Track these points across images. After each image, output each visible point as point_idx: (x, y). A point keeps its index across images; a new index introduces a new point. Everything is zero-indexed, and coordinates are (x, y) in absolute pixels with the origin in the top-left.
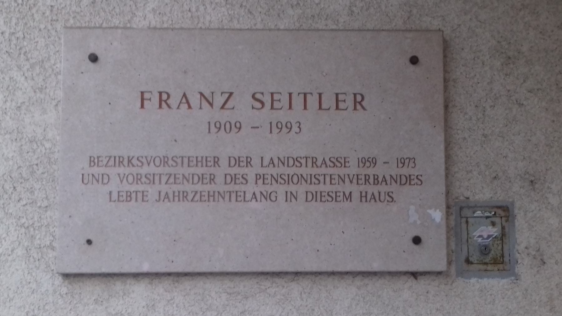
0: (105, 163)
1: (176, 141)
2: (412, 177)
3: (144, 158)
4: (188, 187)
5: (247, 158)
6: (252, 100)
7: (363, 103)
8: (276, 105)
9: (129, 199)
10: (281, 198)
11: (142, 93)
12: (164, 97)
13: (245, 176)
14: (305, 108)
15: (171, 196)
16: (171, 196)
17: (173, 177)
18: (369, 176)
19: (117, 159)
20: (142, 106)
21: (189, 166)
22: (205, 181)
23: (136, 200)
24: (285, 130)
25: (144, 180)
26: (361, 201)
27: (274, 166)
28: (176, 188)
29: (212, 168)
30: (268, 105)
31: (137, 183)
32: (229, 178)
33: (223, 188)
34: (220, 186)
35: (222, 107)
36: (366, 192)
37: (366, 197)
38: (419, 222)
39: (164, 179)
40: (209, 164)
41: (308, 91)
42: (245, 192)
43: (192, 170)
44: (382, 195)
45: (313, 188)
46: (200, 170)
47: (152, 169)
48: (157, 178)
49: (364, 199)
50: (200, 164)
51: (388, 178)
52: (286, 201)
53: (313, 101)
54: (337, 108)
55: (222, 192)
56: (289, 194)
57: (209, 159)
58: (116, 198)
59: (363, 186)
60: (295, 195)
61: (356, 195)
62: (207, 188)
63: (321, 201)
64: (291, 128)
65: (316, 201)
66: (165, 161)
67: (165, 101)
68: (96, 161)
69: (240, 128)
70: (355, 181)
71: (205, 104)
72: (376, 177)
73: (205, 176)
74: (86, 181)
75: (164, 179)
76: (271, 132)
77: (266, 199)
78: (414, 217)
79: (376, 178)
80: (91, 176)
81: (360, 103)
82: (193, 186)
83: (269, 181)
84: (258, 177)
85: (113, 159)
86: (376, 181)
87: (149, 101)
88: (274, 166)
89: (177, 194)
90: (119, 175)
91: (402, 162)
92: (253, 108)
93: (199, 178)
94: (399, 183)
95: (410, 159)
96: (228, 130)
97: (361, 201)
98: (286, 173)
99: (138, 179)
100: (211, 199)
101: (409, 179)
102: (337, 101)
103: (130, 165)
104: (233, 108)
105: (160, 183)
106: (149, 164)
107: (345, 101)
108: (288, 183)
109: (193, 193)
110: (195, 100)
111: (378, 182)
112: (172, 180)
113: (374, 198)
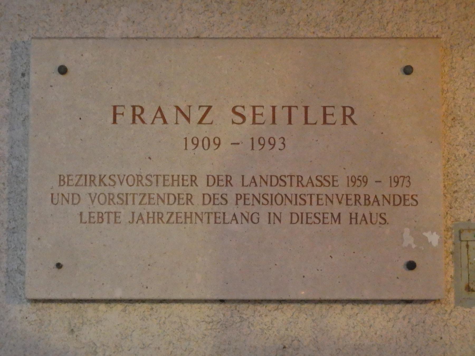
0: (75, 182)
1: (150, 158)
4: (164, 208)
5: (227, 176)
6: (232, 113)
7: (353, 117)
8: (258, 119)
9: (100, 220)
10: (264, 220)
11: (115, 107)
12: (138, 111)
13: (224, 196)
14: (290, 122)
15: (145, 217)
16: (145, 217)
17: (147, 197)
19: (88, 177)
20: (115, 122)
21: (164, 185)
22: (181, 202)
24: (268, 146)
25: (116, 200)
26: (351, 223)
27: (256, 185)
28: (150, 208)
29: (189, 187)
30: (249, 119)
31: (109, 204)
32: (207, 197)
33: (201, 209)
35: (200, 122)
36: (357, 214)
38: (414, 246)
40: (186, 183)
41: (293, 104)
42: (224, 213)
44: (374, 216)
45: (298, 209)
46: (176, 190)
47: (125, 188)
48: (130, 198)
49: (354, 221)
50: (176, 183)
51: (380, 198)
52: (269, 223)
53: (298, 114)
54: (325, 122)
55: (199, 213)
56: (272, 215)
57: (185, 178)
58: (87, 219)
59: (353, 207)
60: (279, 216)
61: (345, 218)
63: (307, 223)
64: (274, 145)
65: (302, 223)
66: (138, 180)
67: (139, 116)
68: (66, 180)
69: (219, 145)
70: (344, 201)
71: (181, 119)
72: (367, 197)
73: (181, 196)
74: (55, 201)
76: (253, 149)
77: (247, 220)
78: (409, 240)
79: (367, 198)
80: (60, 196)
81: (349, 117)
82: (169, 206)
83: (251, 201)
84: (239, 197)
85: (83, 178)
86: (367, 202)
87: (121, 116)
88: (256, 185)
89: (151, 215)
90: (90, 194)
91: (396, 181)
92: (233, 122)
93: (175, 198)
94: (392, 204)
95: (404, 177)
96: (206, 147)
97: (351, 223)
99: (110, 199)
100: (188, 220)
101: (403, 199)
102: (325, 115)
103: (102, 184)
104: (212, 123)
105: (134, 204)
106: (121, 183)
107: (333, 115)
108: (272, 204)
109: (169, 215)
110: (170, 114)
111: (370, 202)
112: (146, 200)
113: (365, 220)
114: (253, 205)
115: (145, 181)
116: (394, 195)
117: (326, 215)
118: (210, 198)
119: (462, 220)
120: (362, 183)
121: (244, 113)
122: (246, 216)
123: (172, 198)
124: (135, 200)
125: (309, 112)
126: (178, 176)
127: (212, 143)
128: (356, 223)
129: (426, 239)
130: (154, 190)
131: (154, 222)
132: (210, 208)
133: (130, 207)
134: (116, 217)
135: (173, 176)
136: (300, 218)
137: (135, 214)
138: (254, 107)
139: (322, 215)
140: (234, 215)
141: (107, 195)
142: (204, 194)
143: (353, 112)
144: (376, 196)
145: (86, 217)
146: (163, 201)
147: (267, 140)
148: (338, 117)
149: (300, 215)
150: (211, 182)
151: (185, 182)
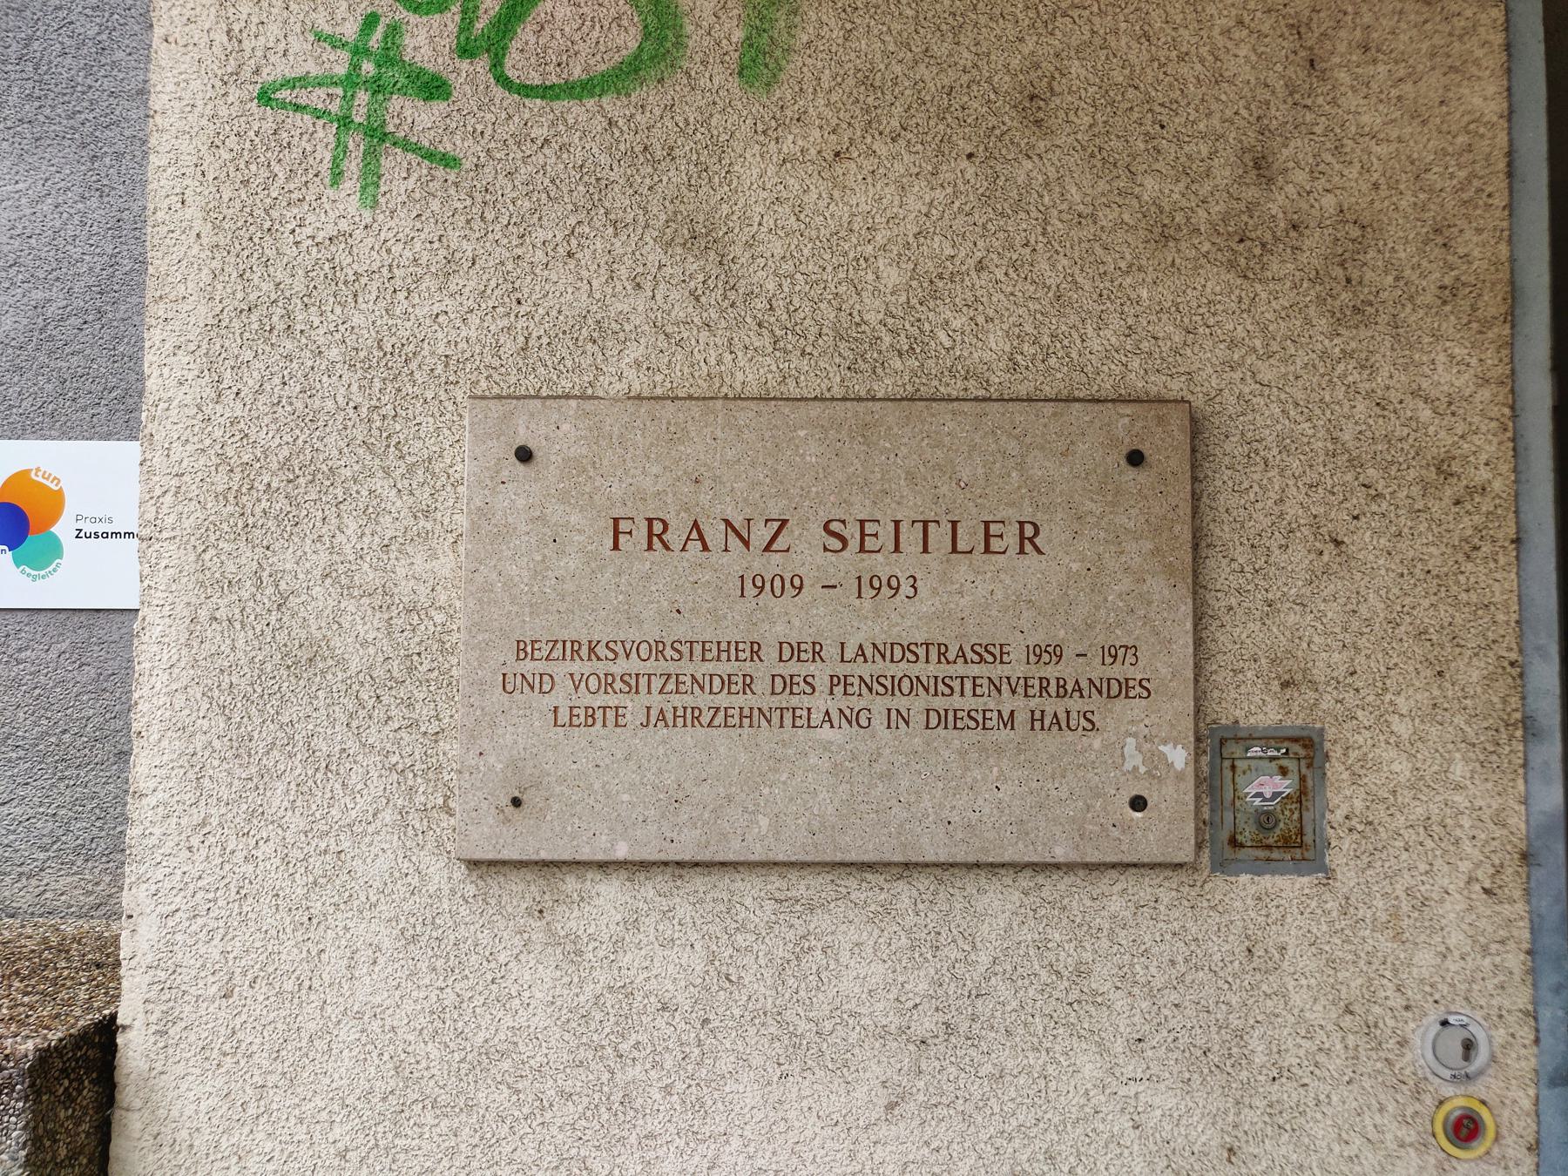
0: (545, 654)
1: (678, 611)
2: (1131, 683)
3: (619, 644)
4: (703, 700)
5: (814, 643)
6: (824, 533)
7: (1037, 541)
8: (870, 543)
9: (590, 721)
10: (879, 722)
11: (616, 521)
12: (658, 528)
13: (809, 679)
14: (925, 550)
15: (669, 716)
16: (669, 716)
17: (673, 680)
18: (1048, 681)
19: (568, 645)
20: (616, 547)
21: (703, 660)
22: (734, 688)
23: (604, 725)
24: (886, 591)
25: (618, 685)
26: (1032, 728)
27: (866, 661)
28: (677, 700)
29: (748, 664)
30: (854, 544)
31: (606, 692)
32: (778, 680)
33: (768, 702)
34: (761, 698)
35: (767, 549)
36: (1043, 712)
37: (1042, 720)
38: (1142, 770)
39: (657, 684)
40: (803, 656)
41: (931, 516)
42: (809, 709)
43: (710, 667)
44: (1074, 715)
45: (939, 703)
46: (724, 668)
47: (634, 665)
48: (643, 681)
49: (1037, 725)
50: (724, 656)
51: (1084, 684)
52: (889, 727)
53: (939, 535)
54: (987, 550)
55: (765, 710)
56: (894, 713)
57: (741, 646)
58: (567, 719)
59: (1037, 700)
60: (906, 716)
61: (1022, 718)
62: (739, 700)
63: (955, 728)
64: (897, 589)
65: (946, 728)
66: (658, 649)
67: (659, 536)
68: (529, 649)
69: (800, 588)
70: (1020, 690)
71: (734, 542)
72: (1062, 683)
73: (734, 679)
74: (509, 688)
75: (657, 684)
76: (860, 596)
77: (850, 723)
78: (1134, 759)
79: (1061, 684)
80: (519, 678)
81: (1031, 540)
82: (712, 697)
83: (856, 688)
84: (835, 679)
85: (560, 645)
86: (1061, 690)
87: (628, 536)
88: (866, 661)
89: (680, 712)
90: (571, 675)
91: (1112, 654)
92: (826, 549)
93: (723, 683)
94: (1105, 695)
95: (1127, 648)
96: (778, 592)
97: (1032, 728)
98: (889, 674)
99: (607, 683)
100: (746, 721)
101: (1125, 686)
102: (987, 536)
103: (593, 656)
104: (788, 550)
105: (649, 692)
106: (628, 656)
107: (1001, 536)
108: (893, 694)
109: (712, 711)
110: (714, 534)
111: (1066, 691)
112: (671, 686)
113: (1058, 723)
114: (860, 695)
115: (669, 652)
116: (1109, 680)
117: (978, 682)
118: (785, 683)
119: (1223, 721)
120: (1054, 658)
121: (846, 533)
122: (849, 715)
123: (717, 681)
124: (652, 686)
125: (960, 531)
126: (729, 643)
127: (788, 585)
128: (1042, 729)
129: (1163, 756)
130: (686, 667)
131: (685, 725)
132: (783, 700)
133: (643, 699)
134: (617, 716)
135: (719, 643)
136: (943, 720)
137: (652, 712)
138: (862, 522)
139: (981, 713)
140: (827, 713)
141: (602, 676)
142: (773, 676)
143: (1037, 532)
144: (1077, 682)
145: (564, 716)
146: (702, 688)
147: (884, 582)
148: (1012, 540)
149: (942, 713)
150: (787, 654)
151: (740, 654)
